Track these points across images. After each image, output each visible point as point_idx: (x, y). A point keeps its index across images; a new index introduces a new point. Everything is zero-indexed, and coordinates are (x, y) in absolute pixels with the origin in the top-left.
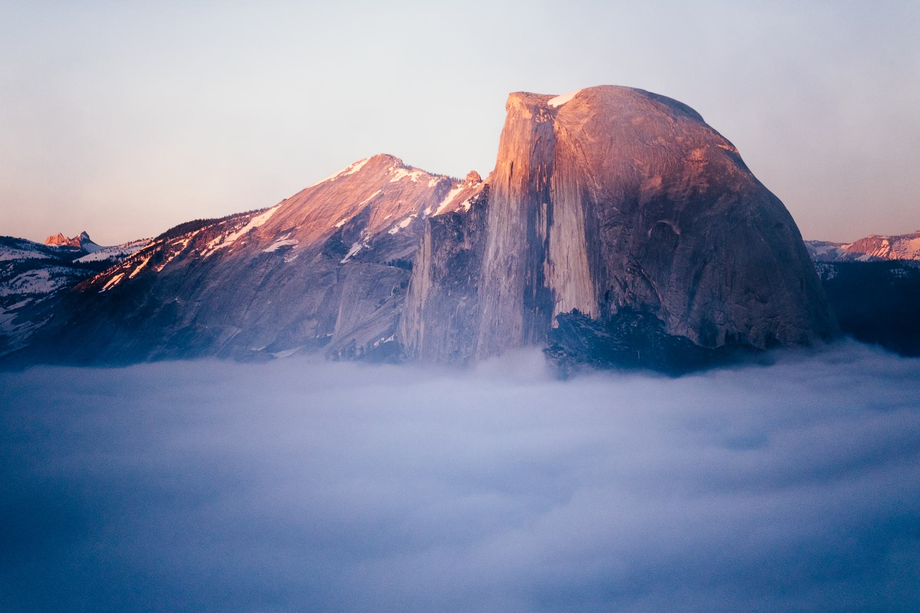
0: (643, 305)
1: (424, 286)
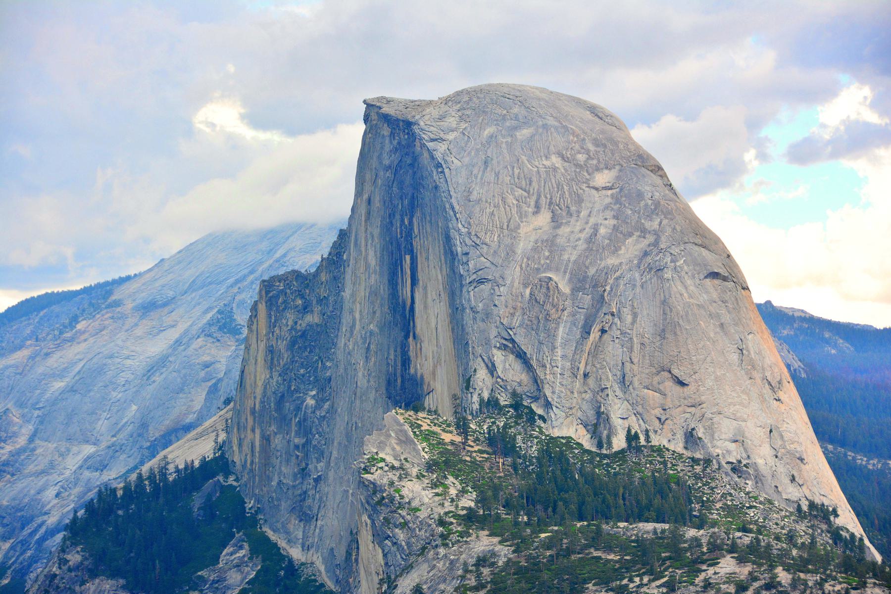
0: (514, 394)
1: (258, 378)
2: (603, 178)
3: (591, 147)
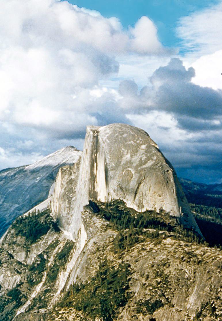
3: (140, 139)
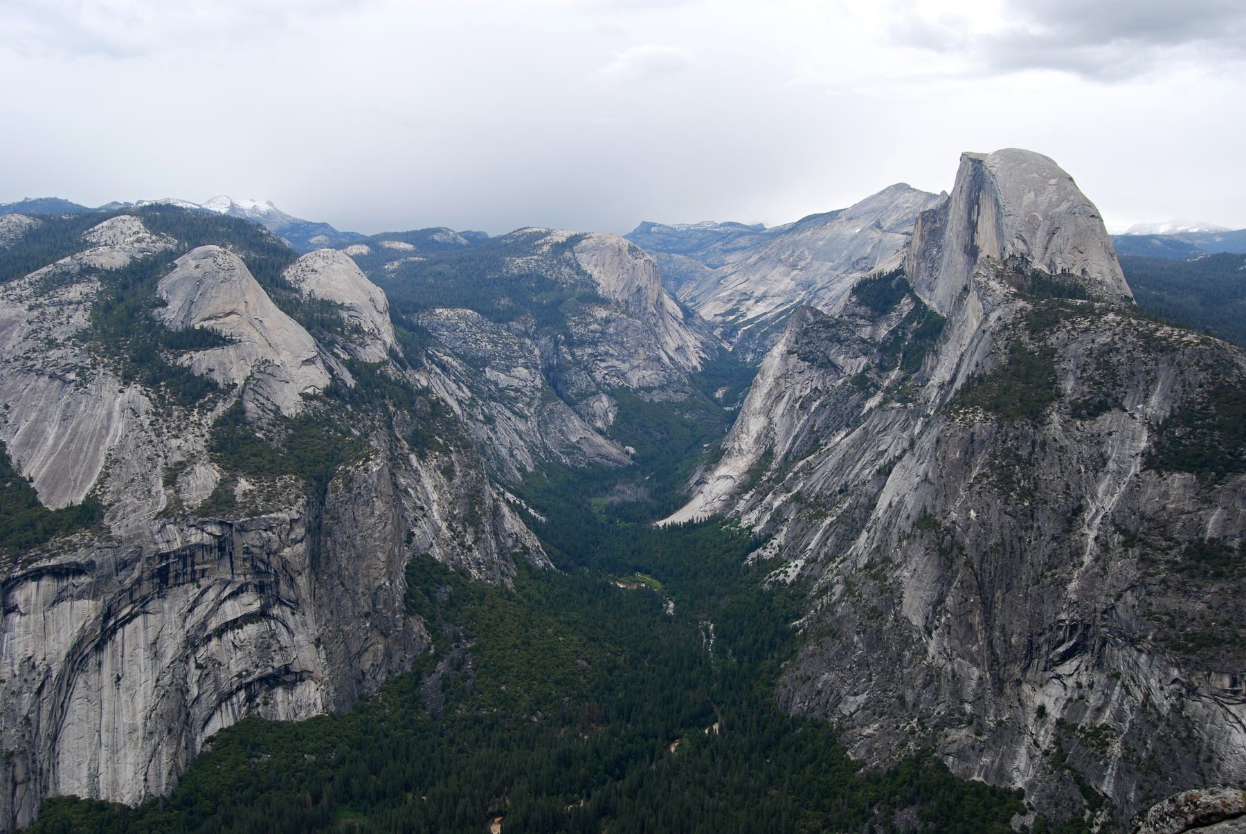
2: (1053, 181)
